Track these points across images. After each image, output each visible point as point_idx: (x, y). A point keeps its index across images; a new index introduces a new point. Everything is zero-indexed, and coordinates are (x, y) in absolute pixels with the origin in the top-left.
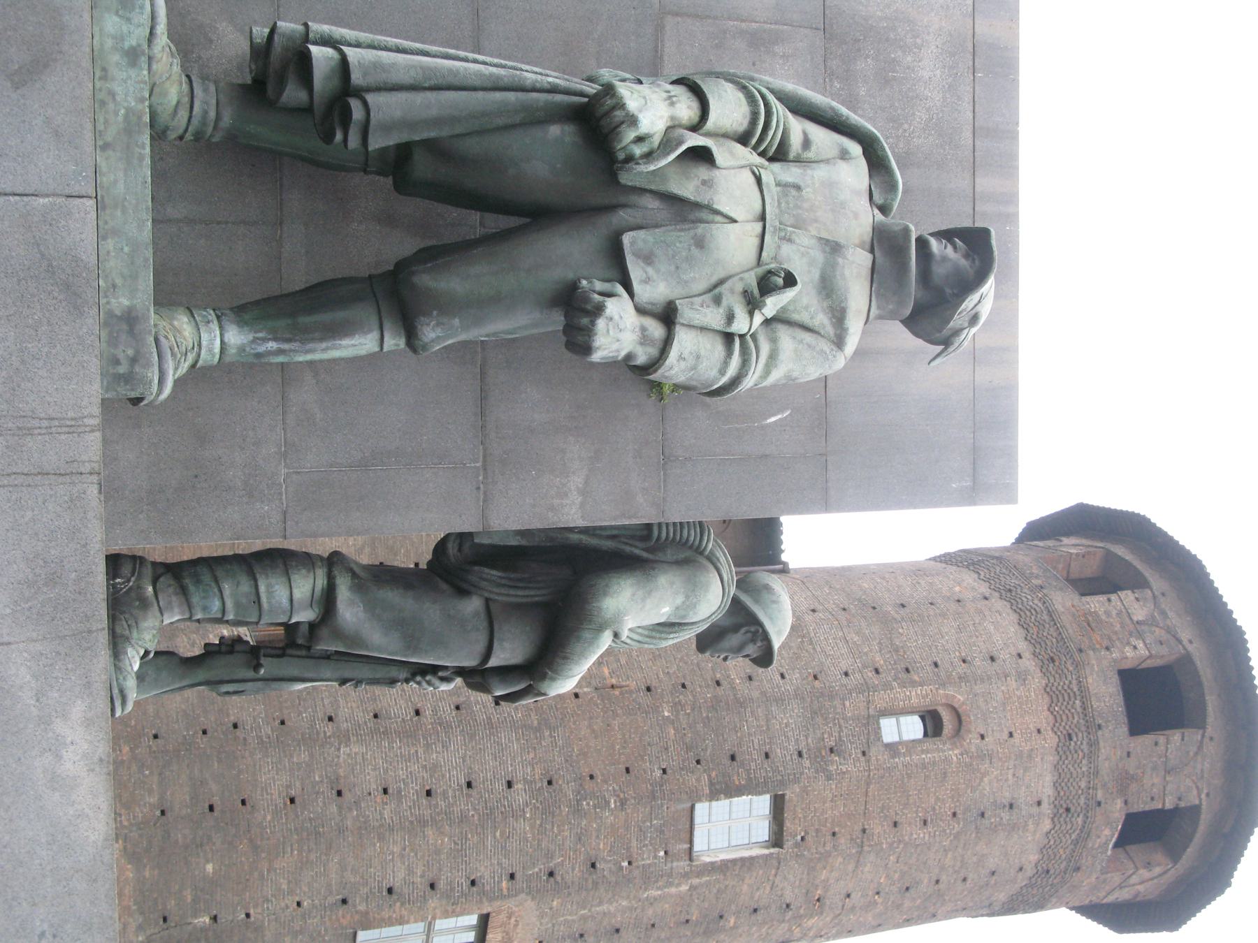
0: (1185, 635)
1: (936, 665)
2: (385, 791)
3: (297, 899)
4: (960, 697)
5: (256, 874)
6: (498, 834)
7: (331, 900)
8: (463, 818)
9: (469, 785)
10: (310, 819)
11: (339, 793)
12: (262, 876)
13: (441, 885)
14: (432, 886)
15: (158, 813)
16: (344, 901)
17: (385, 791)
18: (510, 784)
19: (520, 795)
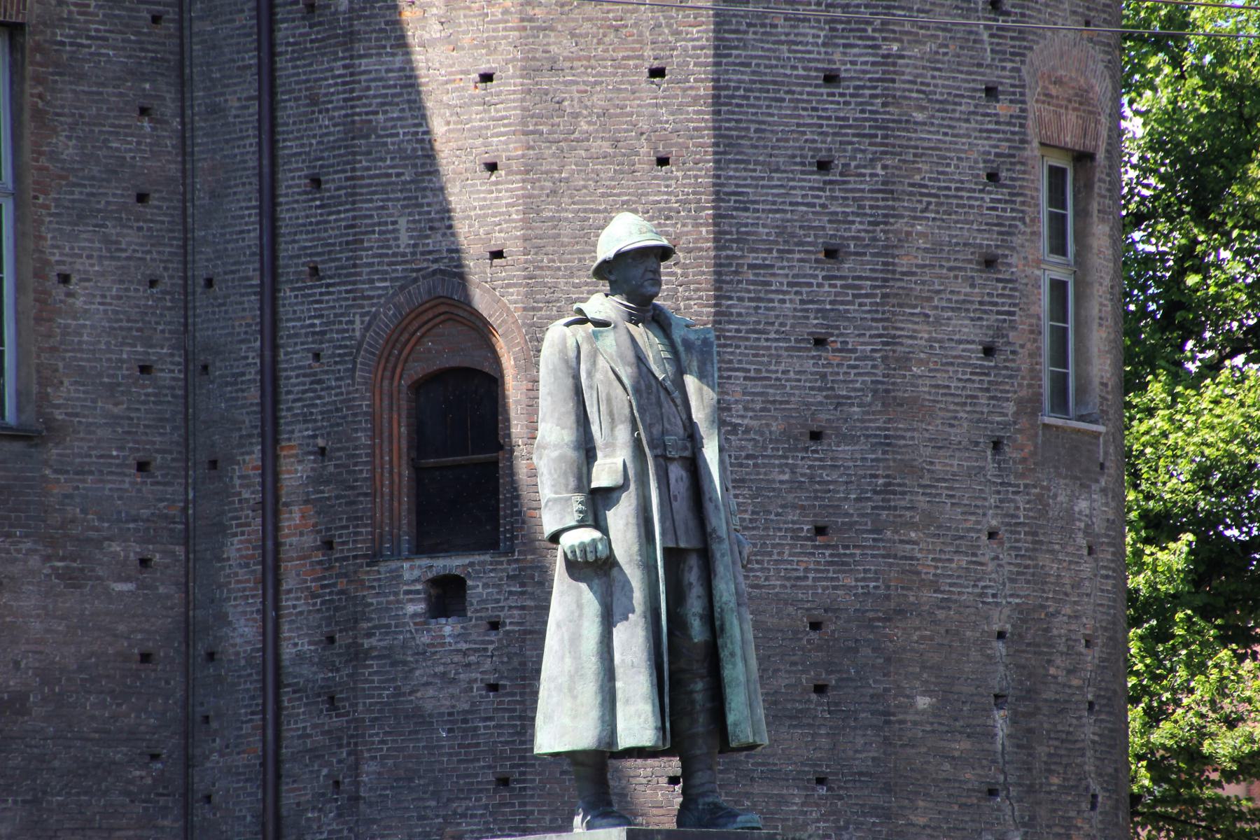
2: (820, 342)
3: (984, 538)
5: (941, 614)
6: (919, 116)
7: (991, 467)
8: (887, 190)
9: (823, 166)
10: (858, 500)
11: (816, 436)
12: (945, 604)
13: (988, 241)
14: (989, 263)
15: (823, 791)
16: (997, 445)
17: (820, 342)
18: (831, 78)
19: (852, 60)
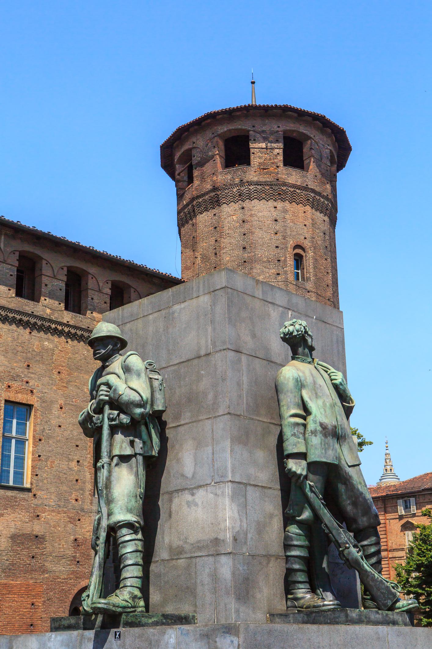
0: (275, 128)
1: (277, 247)
4: (291, 243)
